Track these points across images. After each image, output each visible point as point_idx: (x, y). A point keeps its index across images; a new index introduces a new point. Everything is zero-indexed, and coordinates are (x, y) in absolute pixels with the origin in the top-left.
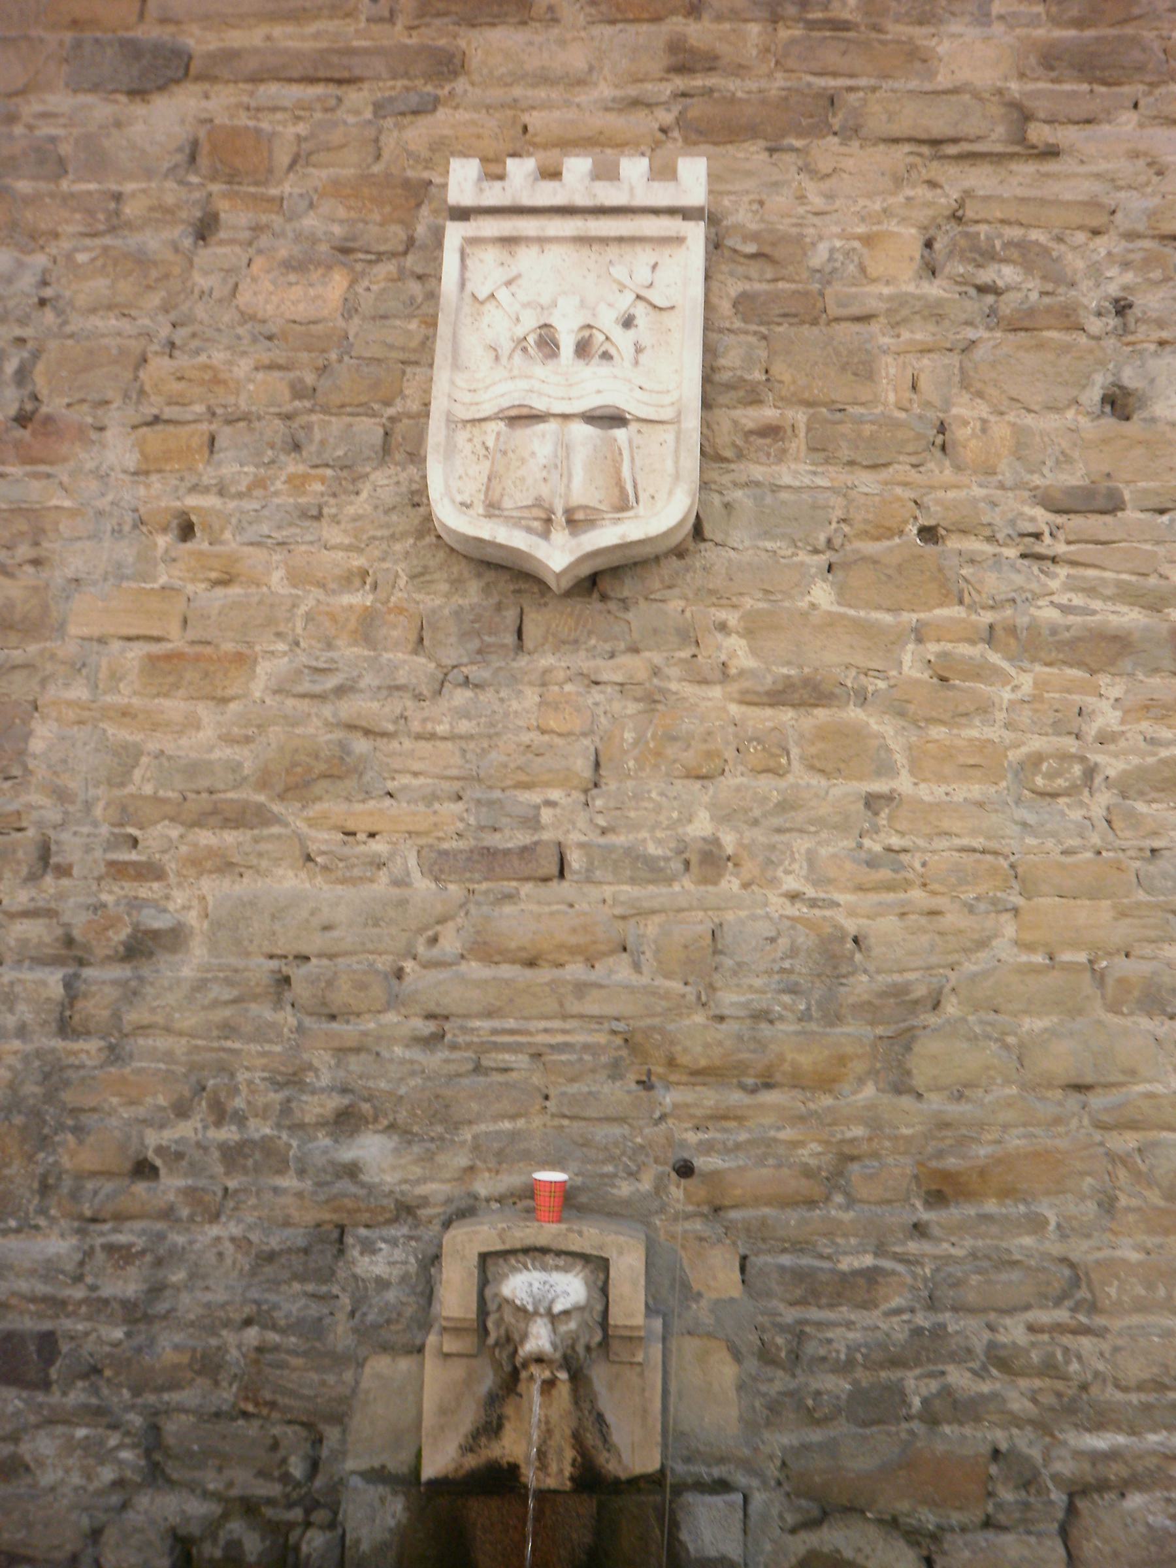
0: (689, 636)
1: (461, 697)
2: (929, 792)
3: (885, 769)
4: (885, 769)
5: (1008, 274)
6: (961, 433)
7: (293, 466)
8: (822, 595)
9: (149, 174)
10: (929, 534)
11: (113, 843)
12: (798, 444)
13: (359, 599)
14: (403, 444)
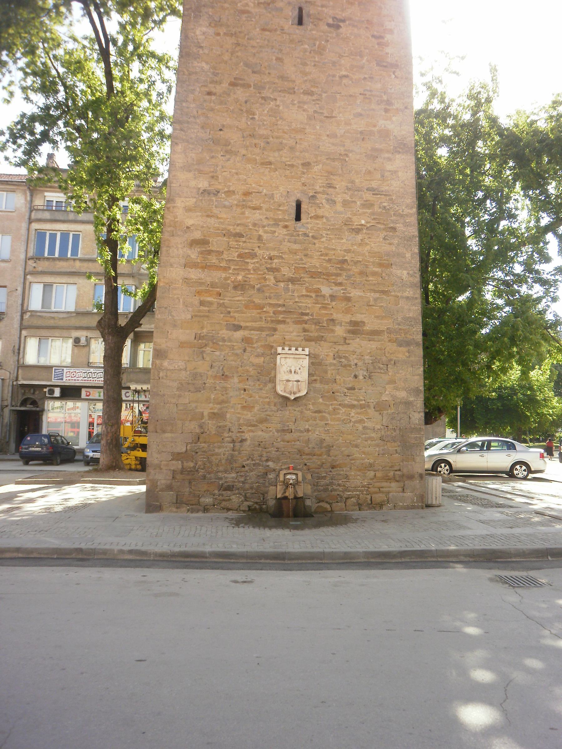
0: (306, 405)
1: (280, 412)
2: (332, 423)
3: (327, 420)
4: (327, 420)
5: (343, 360)
6: (337, 380)
7: (258, 383)
8: (321, 400)
9: (237, 343)
10: (333, 393)
11: (239, 428)
12: (318, 382)
13: (268, 400)
14: (273, 380)
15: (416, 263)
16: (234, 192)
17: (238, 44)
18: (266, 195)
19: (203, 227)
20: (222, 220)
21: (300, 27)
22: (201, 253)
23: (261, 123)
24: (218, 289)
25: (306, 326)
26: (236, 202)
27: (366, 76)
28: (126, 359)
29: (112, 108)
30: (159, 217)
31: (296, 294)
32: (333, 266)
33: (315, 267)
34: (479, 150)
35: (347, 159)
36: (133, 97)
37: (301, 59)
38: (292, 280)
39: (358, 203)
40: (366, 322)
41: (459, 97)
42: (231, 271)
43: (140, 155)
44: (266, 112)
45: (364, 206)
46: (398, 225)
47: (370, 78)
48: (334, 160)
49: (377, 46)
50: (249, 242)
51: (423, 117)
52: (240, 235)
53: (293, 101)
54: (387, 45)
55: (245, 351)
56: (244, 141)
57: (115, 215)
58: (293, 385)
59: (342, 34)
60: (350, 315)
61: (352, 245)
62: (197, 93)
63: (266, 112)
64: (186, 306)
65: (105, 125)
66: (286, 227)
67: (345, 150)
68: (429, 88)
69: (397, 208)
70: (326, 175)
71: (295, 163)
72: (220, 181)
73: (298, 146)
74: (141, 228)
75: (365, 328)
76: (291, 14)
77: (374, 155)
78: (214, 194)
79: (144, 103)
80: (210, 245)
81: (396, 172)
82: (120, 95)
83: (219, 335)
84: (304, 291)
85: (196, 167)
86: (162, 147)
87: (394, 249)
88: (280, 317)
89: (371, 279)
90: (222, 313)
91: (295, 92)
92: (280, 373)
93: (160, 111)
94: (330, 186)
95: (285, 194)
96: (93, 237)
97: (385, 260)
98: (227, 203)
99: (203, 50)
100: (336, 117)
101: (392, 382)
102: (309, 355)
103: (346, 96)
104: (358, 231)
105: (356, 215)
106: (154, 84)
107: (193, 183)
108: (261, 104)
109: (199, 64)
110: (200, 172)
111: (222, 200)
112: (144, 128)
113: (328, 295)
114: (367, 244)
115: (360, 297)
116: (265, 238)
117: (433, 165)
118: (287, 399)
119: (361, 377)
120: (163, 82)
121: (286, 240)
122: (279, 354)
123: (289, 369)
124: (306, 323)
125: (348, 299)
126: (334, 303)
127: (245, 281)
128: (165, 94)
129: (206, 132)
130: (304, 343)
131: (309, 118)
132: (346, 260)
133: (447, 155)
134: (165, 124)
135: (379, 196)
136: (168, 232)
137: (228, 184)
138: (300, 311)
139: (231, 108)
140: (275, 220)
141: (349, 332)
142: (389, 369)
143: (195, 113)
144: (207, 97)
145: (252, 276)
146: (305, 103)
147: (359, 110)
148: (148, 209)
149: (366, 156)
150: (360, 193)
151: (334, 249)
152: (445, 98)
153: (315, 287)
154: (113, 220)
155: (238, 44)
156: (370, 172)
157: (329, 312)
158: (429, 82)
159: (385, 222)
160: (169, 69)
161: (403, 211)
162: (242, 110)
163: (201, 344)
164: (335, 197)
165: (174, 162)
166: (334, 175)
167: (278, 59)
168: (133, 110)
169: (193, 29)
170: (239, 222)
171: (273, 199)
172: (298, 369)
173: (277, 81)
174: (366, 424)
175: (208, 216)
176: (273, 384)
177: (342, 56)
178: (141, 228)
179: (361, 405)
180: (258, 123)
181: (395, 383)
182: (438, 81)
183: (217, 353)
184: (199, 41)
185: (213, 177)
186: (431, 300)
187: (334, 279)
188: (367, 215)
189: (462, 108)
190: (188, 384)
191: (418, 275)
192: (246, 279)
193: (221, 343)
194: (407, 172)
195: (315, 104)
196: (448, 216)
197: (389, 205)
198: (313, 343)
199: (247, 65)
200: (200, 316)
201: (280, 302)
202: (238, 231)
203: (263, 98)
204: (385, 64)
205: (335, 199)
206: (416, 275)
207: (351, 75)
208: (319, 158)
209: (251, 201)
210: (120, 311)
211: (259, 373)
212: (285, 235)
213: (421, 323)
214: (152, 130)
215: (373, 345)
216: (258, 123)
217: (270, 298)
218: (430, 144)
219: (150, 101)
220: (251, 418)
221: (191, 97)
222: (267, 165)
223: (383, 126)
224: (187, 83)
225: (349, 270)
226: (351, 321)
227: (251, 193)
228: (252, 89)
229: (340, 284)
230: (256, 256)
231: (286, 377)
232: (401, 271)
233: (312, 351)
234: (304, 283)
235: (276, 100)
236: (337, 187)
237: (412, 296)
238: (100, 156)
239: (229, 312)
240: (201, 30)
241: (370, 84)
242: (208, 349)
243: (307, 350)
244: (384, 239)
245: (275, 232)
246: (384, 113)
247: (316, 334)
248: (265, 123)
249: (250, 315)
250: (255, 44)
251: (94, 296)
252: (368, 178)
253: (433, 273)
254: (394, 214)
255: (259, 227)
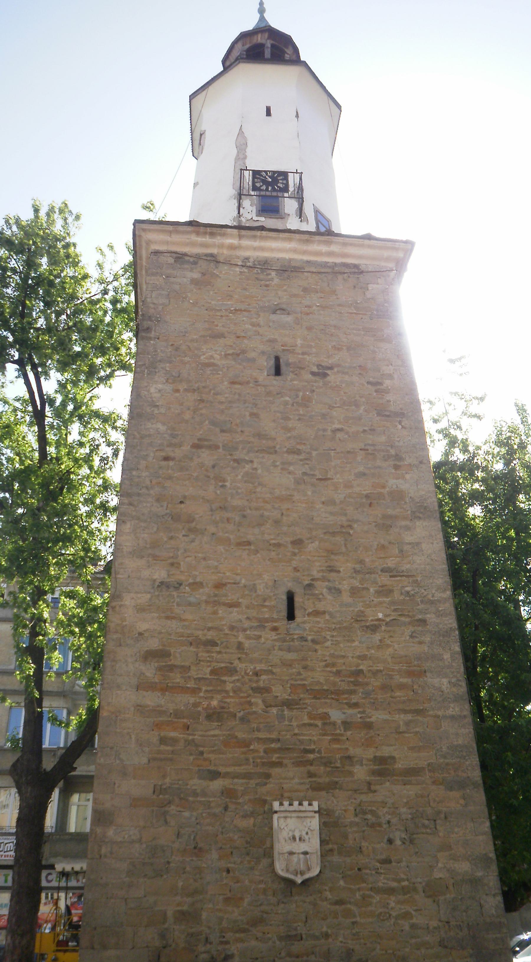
0: (320, 892)
1: (282, 906)
2: (363, 921)
3: (355, 916)
4: (355, 916)
5: (369, 816)
6: (364, 849)
7: (248, 858)
8: (342, 883)
9: (215, 797)
10: (359, 869)
11: (220, 937)
12: (336, 853)
13: (262, 886)
15: (459, 665)
16: (201, 583)
17: (202, 401)
18: (245, 586)
19: (160, 633)
20: (186, 623)
21: (277, 378)
22: (160, 669)
23: (234, 492)
24: (185, 721)
25: (312, 768)
26: (204, 598)
27: (366, 428)
28: (50, 820)
29: (44, 477)
30: (101, 616)
31: (295, 724)
32: (344, 681)
33: (319, 683)
34: (522, 505)
35: (351, 532)
36: (71, 464)
37: (281, 413)
38: (288, 704)
39: (372, 590)
40: (397, 756)
41: (485, 444)
42: (202, 694)
43: (76, 536)
44: (240, 477)
45: (379, 593)
46: (428, 616)
47: (370, 430)
48: (334, 534)
49: (375, 394)
50: (226, 653)
51: (444, 468)
52: (213, 643)
53: (274, 461)
54: (387, 391)
55: (226, 808)
56: (212, 515)
57: (41, 614)
58: (299, 859)
59: (330, 382)
60: (373, 749)
61: (368, 648)
62: (150, 459)
63: (240, 477)
64: (141, 745)
65: (33, 498)
66: (275, 629)
67: (348, 520)
68: (446, 436)
69: (426, 593)
70: (325, 554)
71: (281, 542)
72: (182, 569)
73: (285, 518)
74: (77, 630)
75: (396, 766)
76: (265, 364)
77: (386, 524)
78: (175, 587)
79: (85, 471)
80: (172, 657)
81: (418, 544)
82: (54, 461)
83: (189, 787)
84: (306, 717)
85: (150, 551)
86: (105, 524)
87: (426, 649)
88: (275, 757)
89: (398, 694)
90: (191, 754)
91: (276, 452)
92: (279, 842)
93: (104, 478)
94: (332, 569)
95: (271, 583)
96: (11, 641)
97: (415, 666)
98: (192, 599)
99: (158, 409)
100: (332, 479)
101: (446, 847)
102: (319, 812)
103: (342, 452)
104: (374, 628)
105: (370, 607)
106: (98, 448)
107: (146, 573)
108: (234, 468)
109: (154, 426)
110: (155, 557)
111: (186, 595)
112: (82, 500)
113: (339, 722)
114: (388, 646)
115: (386, 721)
116: (246, 645)
117: (465, 528)
118: (290, 883)
119: (398, 842)
120: (109, 445)
121: (276, 648)
122: (276, 812)
123: (291, 834)
124: (311, 765)
125: (369, 726)
126: (349, 733)
127: (223, 708)
128: (110, 459)
129: (162, 506)
130: (310, 793)
131: (298, 482)
132: (361, 671)
133: (482, 515)
134: (109, 494)
135: (399, 578)
136: (113, 640)
137: (194, 573)
138: (302, 747)
139: (195, 474)
140: (259, 620)
141: (374, 773)
142: (438, 827)
143: (148, 483)
144: (164, 463)
145: (232, 700)
146: (290, 464)
147: (361, 469)
148: (85, 605)
149: (376, 526)
150: (373, 576)
151: (344, 657)
152: (468, 446)
153: (321, 711)
154: (39, 620)
155: (202, 401)
156: (383, 547)
157: (343, 747)
158: (446, 429)
159: (410, 614)
160: (117, 430)
161: (433, 596)
162: (209, 477)
163: (163, 800)
164: (340, 584)
165: (120, 545)
166: (336, 554)
167: (252, 415)
168: (69, 479)
169: (146, 387)
170: (210, 625)
171: (256, 592)
172: (304, 833)
173: (252, 439)
174: (414, 921)
175: (168, 618)
176: (270, 860)
177: (334, 407)
178: (77, 630)
179: (403, 888)
180: (230, 491)
181: (450, 848)
182: (455, 427)
183: (187, 814)
184: (154, 399)
185: (172, 564)
186: (486, 712)
187: (346, 699)
188: (385, 605)
189: (490, 456)
190: (144, 864)
191: (464, 684)
192: (223, 705)
193: (191, 799)
194: (432, 543)
195: (303, 465)
196: (495, 596)
197: (414, 590)
198: (323, 793)
199: (213, 423)
200: (161, 760)
201: (274, 736)
202: (209, 637)
203: (235, 461)
204: (387, 413)
205: (340, 587)
206: (460, 683)
207: (346, 428)
208: (314, 533)
209: (226, 596)
210: (46, 745)
211: (247, 842)
212: (275, 640)
213: (476, 753)
214: (93, 503)
215: (411, 791)
216: (230, 491)
217: (259, 730)
218: (458, 504)
219: (91, 468)
220: (240, 918)
221: (143, 463)
222: (245, 546)
223: (394, 487)
224: (138, 448)
225: (367, 684)
226: (375, 757)
227: (225, 585)
228: (220, 450)
229: (356, 705)
230: (237, 671)
231: (287, 848)
232: (438, 679)
233: (323, 806)
234: (304, 706)
235: (252, 462)
236: (341, 569)
237: (459, 713)
238: (25, 536)
239: (202, 753)
240: (157, 388)
241: (371, 437)
242: (173, 809)
243: (316, 804)
244: (411, 636)
245: (260, 637)
246: (393, 471)
247: (327, 780)
248: (240, 491)
249: (231, 756)
250: (223, 399)
251: (8, 723)
252: (382, 556)
253: (485, 673)
254: (422, 602)
255: (238, 631)
